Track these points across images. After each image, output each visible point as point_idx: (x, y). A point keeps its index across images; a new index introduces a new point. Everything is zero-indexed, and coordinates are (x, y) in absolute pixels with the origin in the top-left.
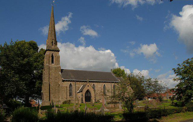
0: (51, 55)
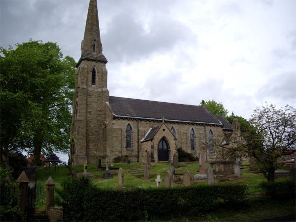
0: (91, 69)
